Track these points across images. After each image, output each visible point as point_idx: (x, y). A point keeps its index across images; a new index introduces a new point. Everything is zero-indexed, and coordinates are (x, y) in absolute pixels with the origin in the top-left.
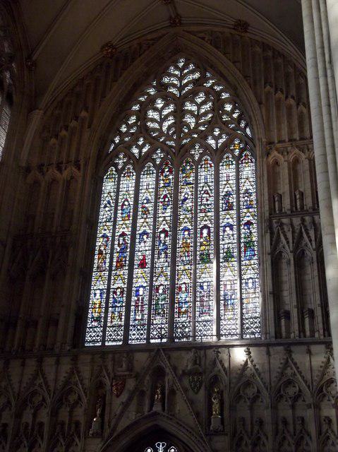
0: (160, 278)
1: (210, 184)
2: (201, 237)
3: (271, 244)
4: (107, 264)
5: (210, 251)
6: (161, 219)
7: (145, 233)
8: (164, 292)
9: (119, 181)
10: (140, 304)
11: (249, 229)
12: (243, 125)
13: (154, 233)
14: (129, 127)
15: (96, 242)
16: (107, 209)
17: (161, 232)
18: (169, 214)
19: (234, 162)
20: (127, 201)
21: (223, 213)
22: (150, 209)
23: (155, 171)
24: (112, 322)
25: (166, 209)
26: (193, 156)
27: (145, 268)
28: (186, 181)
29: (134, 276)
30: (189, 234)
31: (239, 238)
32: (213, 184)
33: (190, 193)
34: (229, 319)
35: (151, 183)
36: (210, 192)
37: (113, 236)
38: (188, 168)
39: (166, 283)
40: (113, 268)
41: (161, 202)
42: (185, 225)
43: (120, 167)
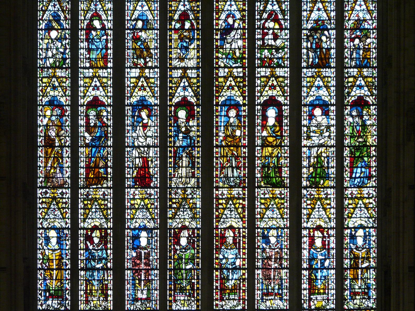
2: (264, 127)
5: (282, 161)
6: (177, 73)
10: (143, 266)
13: (163, 106)
15: (34, 116)
16: (54, 34)
17: (179, 105)
20: (100, 19)
22: (152, 45)
24: (87, 302)
25: (187, 49)
30: (238, 116)
31: (340, 136)
33: (238, 15)
36: (280, 17)
37: (74, 105)
40: (81, 183)
41: (176, 31)
42: (228, 93)
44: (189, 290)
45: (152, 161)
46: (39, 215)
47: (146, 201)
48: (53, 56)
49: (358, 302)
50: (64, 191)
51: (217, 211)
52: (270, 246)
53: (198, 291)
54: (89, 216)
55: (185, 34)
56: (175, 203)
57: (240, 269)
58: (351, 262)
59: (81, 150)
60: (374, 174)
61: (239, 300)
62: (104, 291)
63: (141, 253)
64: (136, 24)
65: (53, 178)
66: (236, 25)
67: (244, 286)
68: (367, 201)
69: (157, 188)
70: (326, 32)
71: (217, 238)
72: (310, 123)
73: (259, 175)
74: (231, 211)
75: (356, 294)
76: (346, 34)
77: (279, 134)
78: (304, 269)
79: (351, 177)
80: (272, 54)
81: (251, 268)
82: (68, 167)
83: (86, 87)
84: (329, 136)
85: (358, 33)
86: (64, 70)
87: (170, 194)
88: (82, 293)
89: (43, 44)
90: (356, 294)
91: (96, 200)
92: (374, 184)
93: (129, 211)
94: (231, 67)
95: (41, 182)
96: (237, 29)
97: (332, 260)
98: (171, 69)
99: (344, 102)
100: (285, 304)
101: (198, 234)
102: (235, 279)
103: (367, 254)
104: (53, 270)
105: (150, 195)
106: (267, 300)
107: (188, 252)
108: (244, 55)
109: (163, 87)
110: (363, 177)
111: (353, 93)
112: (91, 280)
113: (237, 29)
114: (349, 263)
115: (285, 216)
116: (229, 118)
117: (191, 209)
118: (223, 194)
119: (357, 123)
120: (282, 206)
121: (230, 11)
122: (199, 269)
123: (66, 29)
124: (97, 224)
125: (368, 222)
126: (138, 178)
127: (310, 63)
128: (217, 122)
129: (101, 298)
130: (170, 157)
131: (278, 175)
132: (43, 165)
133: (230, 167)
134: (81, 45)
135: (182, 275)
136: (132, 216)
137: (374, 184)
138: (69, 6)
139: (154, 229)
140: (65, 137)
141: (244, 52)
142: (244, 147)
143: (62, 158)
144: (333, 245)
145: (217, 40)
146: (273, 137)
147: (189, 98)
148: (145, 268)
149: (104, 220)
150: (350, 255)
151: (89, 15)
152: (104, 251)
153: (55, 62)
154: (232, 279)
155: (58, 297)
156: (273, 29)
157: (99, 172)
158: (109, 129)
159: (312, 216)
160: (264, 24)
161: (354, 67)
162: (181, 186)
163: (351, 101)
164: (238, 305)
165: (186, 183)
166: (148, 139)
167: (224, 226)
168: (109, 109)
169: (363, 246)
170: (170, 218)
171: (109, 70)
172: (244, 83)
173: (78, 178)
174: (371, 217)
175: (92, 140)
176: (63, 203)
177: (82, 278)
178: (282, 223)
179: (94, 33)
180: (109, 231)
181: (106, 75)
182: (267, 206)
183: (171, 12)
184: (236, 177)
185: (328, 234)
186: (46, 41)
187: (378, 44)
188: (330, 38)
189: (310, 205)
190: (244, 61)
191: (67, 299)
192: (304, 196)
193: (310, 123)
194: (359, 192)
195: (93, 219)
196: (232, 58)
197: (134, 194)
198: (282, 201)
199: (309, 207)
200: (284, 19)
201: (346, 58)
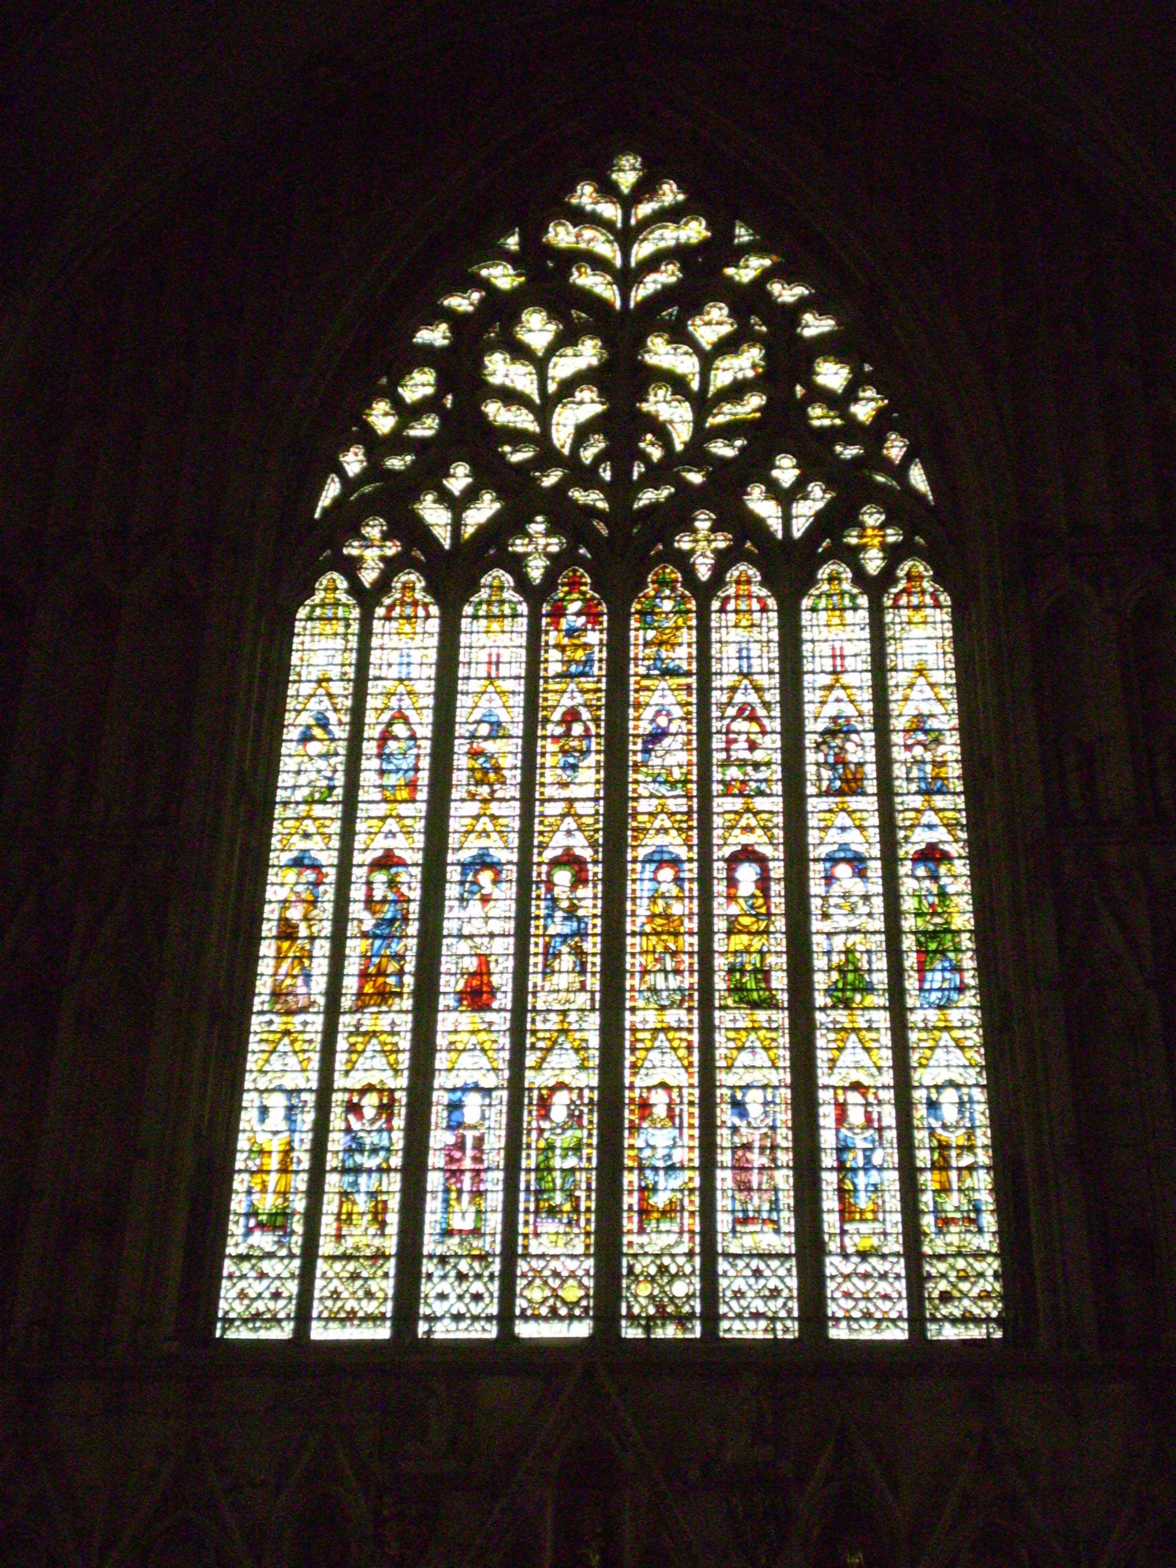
0: (554, 1059)
1: (764, 681)
4: (319, 984)
5: (771, 960)
7: (482, 862)
8: (575, 1119)
9: (366, 634)
10: (467, 1164)
11: (935, 877)
12: (895, 449)
13: (525, 864)
14: (408, 413)
16: (314, 748)
17: (555, 863)
18: (589, 791)
20: (406, 721)
22: (507, 762)
23: (523, 608)
24: (339, 1237)
25: (574, 767)
26: (683, 561)
27: (487, 1008)
28: (658, 658)
29: (441, 1041)
30: (678, 880)
31: (893, 914)
32: (776, 680)
33: (678, 712)
34: (863, 1255)
35: (506, 655)
36: (761, 712)
38: (668, 605)
40: (346, 1002)
41: (555, 738)
43: (368, 577)
44: (568, 1212)
45: (496, 961)
47: (483, 1036)
51: (633, 1050)
52: (749, 1123)
53: (588, 1216)
54: (357, 1066)
55: (572, 744)
56: (544, 1039)
57: (682, 1168)
58: (932, 1155)
59: (349, 943)
61: (681, 1233)
62: (378, 1217)
63: (463, 1137)
64: (476, 730)
65: (287, 994)
66: (673, 728)
67: (692, 1202)
69: (505, 1010)
70: (854, 737)
71: (632, 1107)
75: (948, 1222)
77: (763, 910)
78: (827, 1169)
79: (921, 989)
80: (745, 774)
81: (708, 1167)
83: (370, 833)
84: (870, 915)
86: (329, 806)
87: (533, 1021)
89: (287, 764)
90: (948, 1222)
91: (374, 1034)
94: (663, 797)
95: (263, 1003)
96: (675, 734)
97: (889, 1151)
98: (543, 802)
101: (591, 1099)
102: (673, 1190)
103: (969, 1139)
104: (268, 1172)
105: (491, 1024)
106: (745, 1233)
107: (569, 1133)
108: (690, 777)
109: (526, 833)
110: (949, 989)
112: (352, 1193)
113: (675, 734)
114: (929, 1157)
116: (659, 883)
117: (577, 1050)
118: (645, 1021)
120: (774, 1044)
121: (663, 705)
122: (592, 1169)
123: (340, 739)
124: (375, 1081)
125: (966, 1075)
126: (466, 992)
127: (824, 788)
128: (634, 891)
130: (536, 954)
131: (763, 985)
133: (660, 971)
134: (365, 764)
135: (553, 1180)
136: (449, 1066)
138: (349, 703)
139: (496, 1088)
140: (321, 920)
141: (689, 773)
142: (691, 933)
143: (310, 957)
145: (635, 753)
146: (751, 915)
147: (578, 852)
148: (472, 1167)
149: (391, 1073)
150: (930, 1141)
151: (386, 717)
152: (385, 1135)
153: (312, 794)
154: (666, 1189)
155: (274, 1228)
156: (748, 733)
157: (385, 983)
159: (838, 1064)
161: (917, 793)
163: (912, 852)
164: (677, 1243)
169: (957, 1122)
170: (531, 1068)
171: (417, 805)
172: (690, 823)
174: (971, 1066)
175: (377, 926)
176: (305, 1041)
177: (332, 1190)
178: (774, 1077)
180: (398, 1095)
181: (413, 814)
182: (739, 1044)
183: (545, 708)
184: (674, 990)
185: (876, 1097)
186: (299, 759)
187: (962, 753)
188: (863, 746)
189: (835, 1041)
190: (689, 786)
191: (293, 1233)
192: (821, 1024)
193: (827, 892)
194: (942, 1017)
196: (665, 782)
200: (770, 717)
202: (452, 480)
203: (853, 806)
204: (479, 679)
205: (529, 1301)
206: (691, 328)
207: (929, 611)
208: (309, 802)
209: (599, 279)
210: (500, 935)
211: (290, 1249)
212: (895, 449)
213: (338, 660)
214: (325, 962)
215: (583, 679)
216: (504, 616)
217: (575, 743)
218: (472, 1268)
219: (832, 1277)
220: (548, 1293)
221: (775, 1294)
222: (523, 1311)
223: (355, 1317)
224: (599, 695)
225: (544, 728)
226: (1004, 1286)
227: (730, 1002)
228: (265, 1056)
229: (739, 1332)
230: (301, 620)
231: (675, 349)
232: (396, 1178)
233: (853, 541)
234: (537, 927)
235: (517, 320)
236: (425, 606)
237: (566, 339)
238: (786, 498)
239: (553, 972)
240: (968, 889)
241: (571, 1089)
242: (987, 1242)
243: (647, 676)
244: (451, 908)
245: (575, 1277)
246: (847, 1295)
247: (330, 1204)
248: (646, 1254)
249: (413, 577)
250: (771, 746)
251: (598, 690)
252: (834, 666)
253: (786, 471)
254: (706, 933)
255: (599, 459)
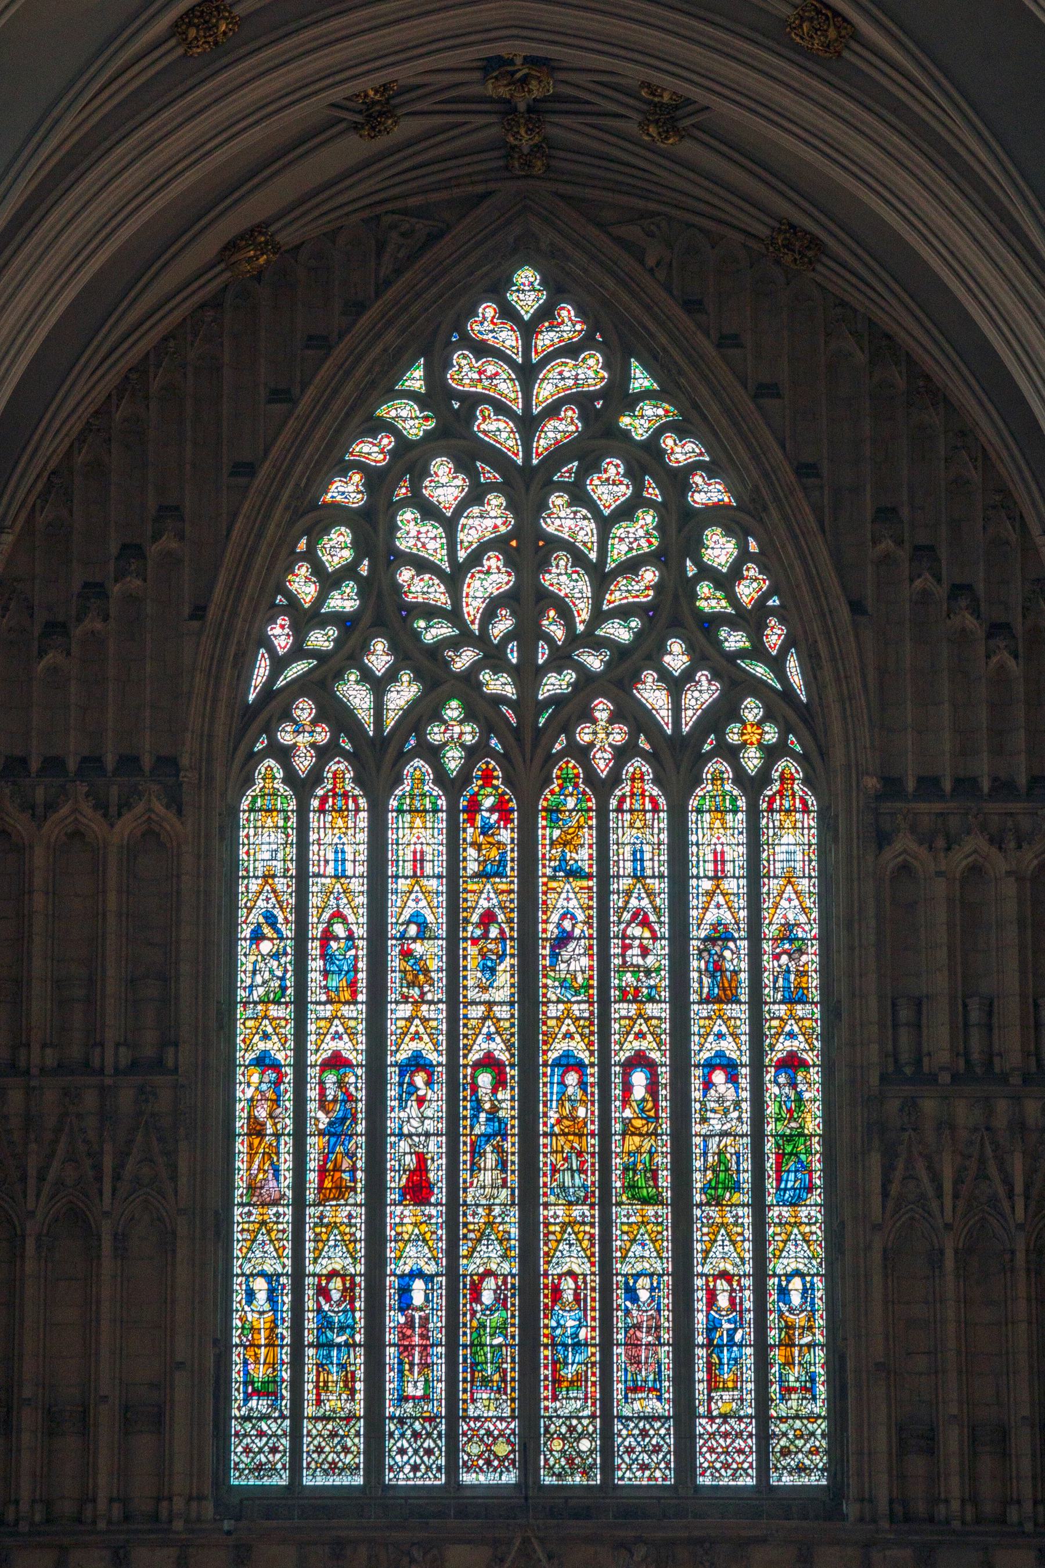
1: (655, 884)
2: (626, 1101)
3: (885, 1194)
4: (287, 1179)
5: (658, 1159)
7: (417, 1063)
8: (501, 1301)
9: (303, 828)
10: (417, 1339)
11: (793, 1085)
12: (774, 636)
13: (453, 1066)
14: (329, 582)
16: (266, 947)
17: (477, 1065)
19: (742, 803)
20: (344, 920)
21: (704, 1010)
22: (433, 965)
23: (442, 803)
24: (319, 1402)
25: (493, 971)
26: (582, 753)
28: (563, 859)
29: (390, 1233)
30: (582, 1084)
32: (665, 885)
33: (581, 916)
34: (725, 1417)
36: (652, 918)
39: (506, 1268)
40: (310, 1196)
43: (303, 763)
45: (432, 1159)
46: (236, 1253)
47: (424, 1228)
48: (264, 982)
49: (794, 1404)
50: (281, 1210)
51: (546, 1244)
56: (473, 1231)
57: (586, 1345)
59: (311, 1140)
60: (818, 1182)
61: (586, 1399)
63: (413, 1317)
64: (405, 930)
65: (262, 1188)
66: (577, 932)
68: (807, 1229)
69: (441, 1205)
70: (731, 945)
72: (705, 1096)
73: (618, 1184)
74: (571, 1245)
75: (791, 1390)
76: (765, 946)
77: (652, 1113)
78: (699, 1346)
79: (778, 1188)
80: (639, 980)
81: (606, 1345)
82: (288, 1170)
84: (739, 1119)
85: (787, 946)
87: (465, 1215)
88: (310, 1386)
89: (246, 963)
90: (791, 1390)
91: (336, 1225)
92: (819, 1201)
93: (393, 1244)
94: (569, 1001)
95: (241, 1196)
96: (579, 939)
99: (763, 1061)
100: (667, 1407)
101: (513, 1285)
104: (259, 1346)
105: (430, 1217)
111: (779, 1046)
113: (579, 939)
115: (665, 1255)
116: (566, 1086)
119: (787, 1096)
124: (338, 1267)
128: (545, 1094)
129: (344, 1396)
130: (465, 1153)
132: (245, 1166)
135: (485, 1354)
136: (398, 1254)
137: (819, 1201)
138: (293, 901)
139: (437, 1275)
141: (591, 977)
142: (592, 1134)
143: (278, 1154)
144: (748, 1305)
145: (544, 957)
147: (496, 1053)
149: (350, 1260)
151: (326, 916)
153: (267, 994)
155: (268, 1394)
156: (641, 938)
158: (360, 1105)
160: (625, 930)
161: (781, 1002)
162: (483, 1202)
164: (584, 1408)
165: (492, 1197)
166: (427, 1122)
167: (559, 1271)
168: (360, 1071)
170: (464, 1257)
171: (359, 1007)
173: (305, 1189)
174: (814, 1257)
175: (330, 1124)
176: (278, 1231)
179: (334, 945)
180: (358, 1279)
181: (355, 1015)
183: (465, 910)
185: (739, 1284)
189: (707, 1234)
191: (283, 1398)
193: (705, 1096)
195: (329, 1258)
196: (571, 987)
197: (402, 1217)
198: (659, 1229)
199: (706, 1238)
200: (660, 923)
201: (766, 986)
202: (373, 658)
203: (728, 1013)
204: (406, 878)
205: (469, 1455)
206: (589, 488)
207: (799, 816)
208: (264, 1001)
209: (502, 425)
210: (434, 1134)
211: (281, 1411)
212: (774, 636)
213: (280, 856)
214: (289, 1158)
215: (498, 880)
216: (425, 811)
217: (492, 946)
218: (424, 1428)
219: (701, 1436)
220: (483, 1448)
221: (657, 1449)
222: (465, 1463)
223: (336, 1467)
224: (512, 896)
225: (465, 930)
226: (828, 1443)
227: (624, 1198)
228: (248, 1244)
229: (630, 1479)
230: (244, 811)
231: (575, 513)
232: (360, 1351)
233: (733, 738)
234: (465, 1127)
235: (425, 473)
236: (355, 799)
237: (476, 496)
238: (676, 686)
239: (480, 1170)
240: (819, 1097)
241: (496, 1276)
242: (819, 1408)
243: (553, 878)
244: (392, 1109)
245: (503, 1436)
246: (712, 1450)
247: (310, 1375)
248: (559, 1417)
249: (342, 767)
250: (660, 955)
251: (511, 891)
252: (716, 871)
253: (676, 658)
254: (605, 1135)
255: (507, 638)
